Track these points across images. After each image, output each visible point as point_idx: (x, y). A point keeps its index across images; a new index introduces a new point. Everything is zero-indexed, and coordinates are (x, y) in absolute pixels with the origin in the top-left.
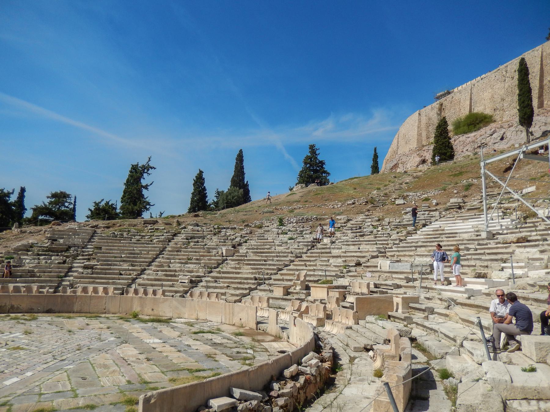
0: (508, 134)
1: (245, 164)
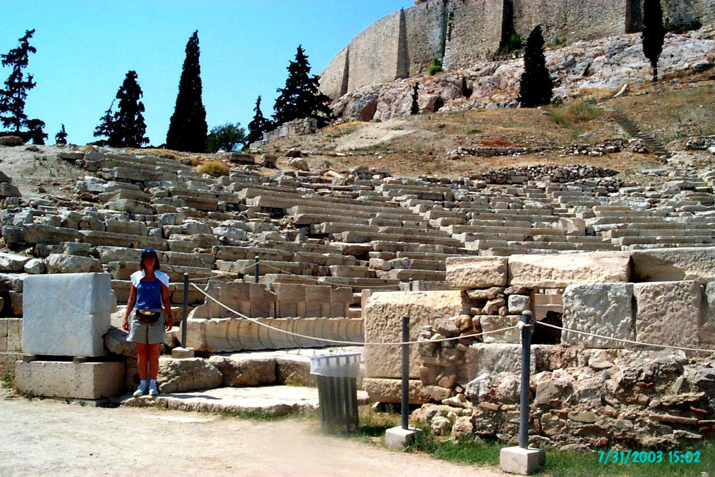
0: (595, 66)
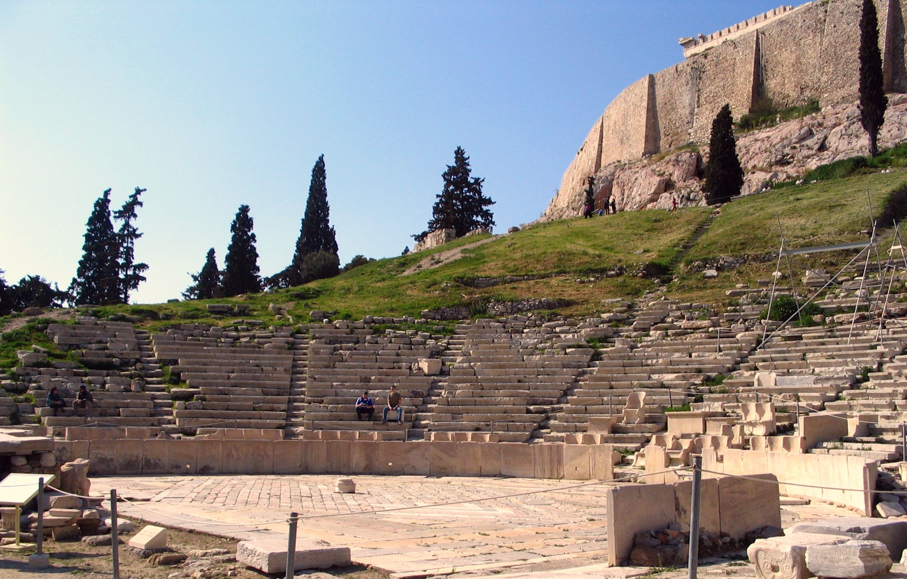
1: (329, 184)
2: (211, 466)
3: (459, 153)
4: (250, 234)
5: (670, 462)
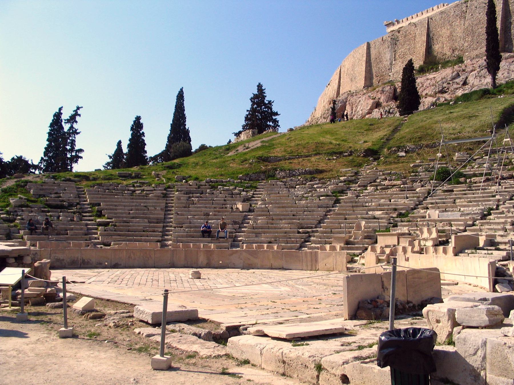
1: (186, 104)
2: (119, 263)
3: (260, 87)
4: (141, 132)
5: (379, 261)
